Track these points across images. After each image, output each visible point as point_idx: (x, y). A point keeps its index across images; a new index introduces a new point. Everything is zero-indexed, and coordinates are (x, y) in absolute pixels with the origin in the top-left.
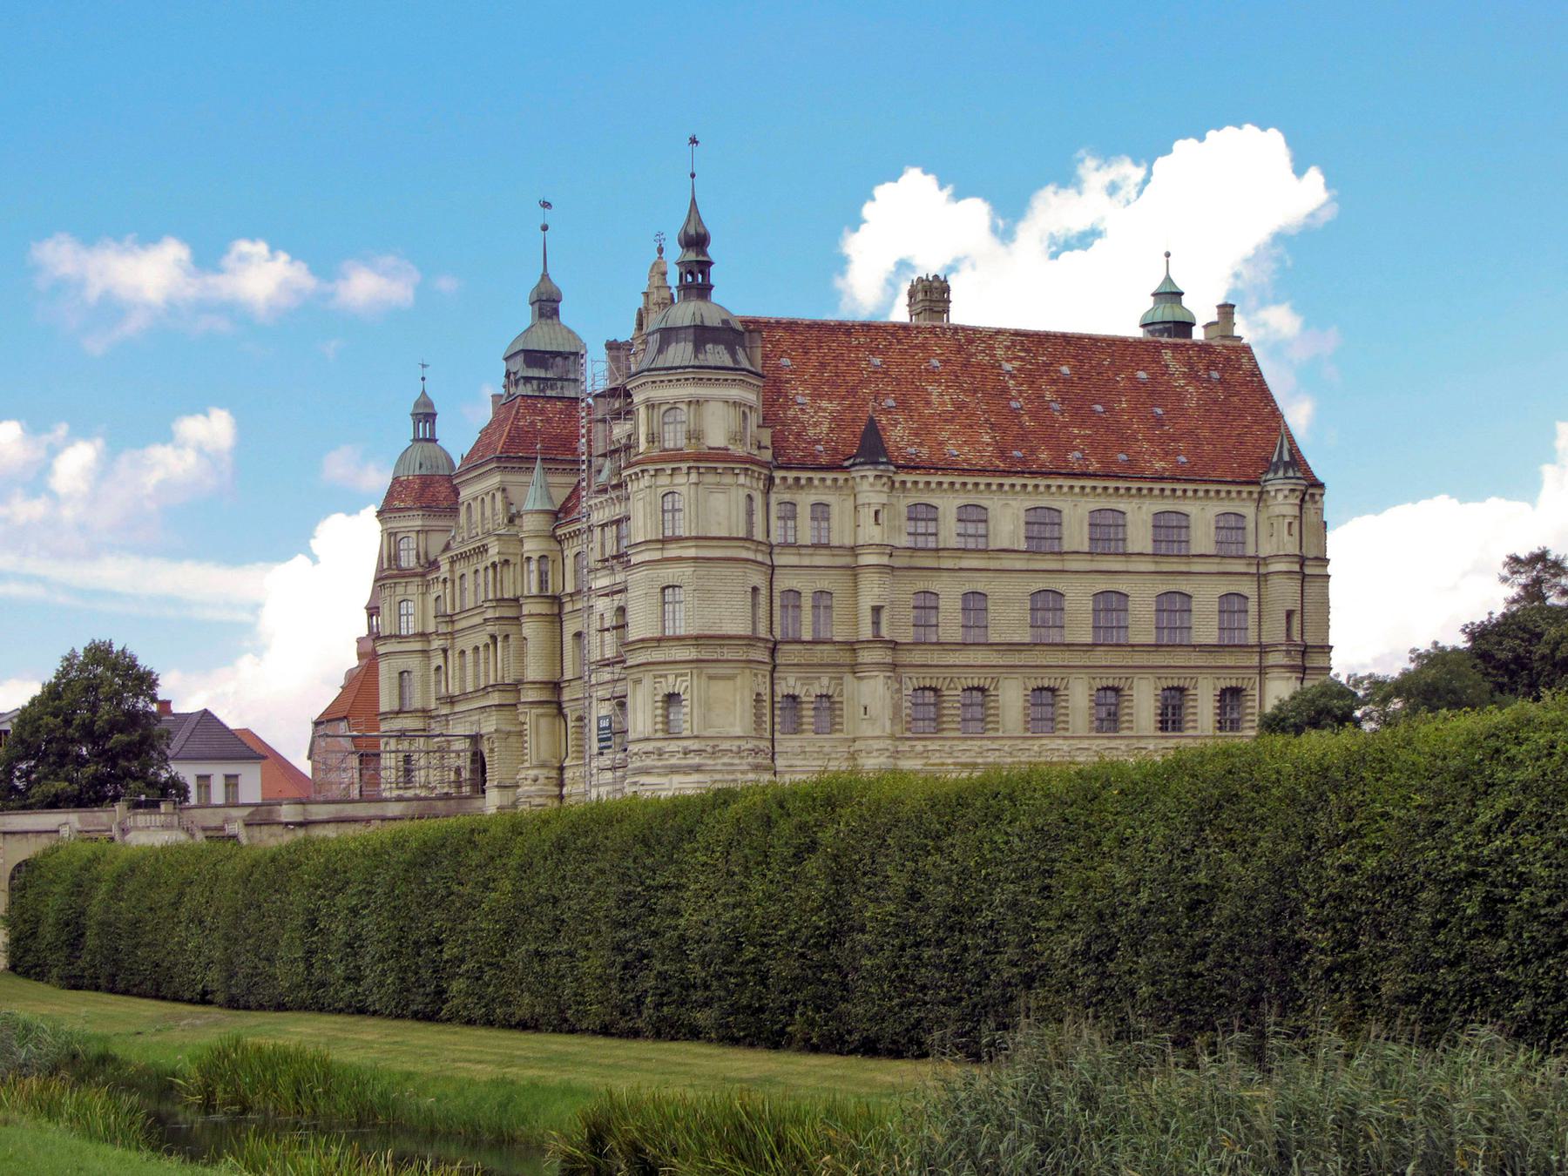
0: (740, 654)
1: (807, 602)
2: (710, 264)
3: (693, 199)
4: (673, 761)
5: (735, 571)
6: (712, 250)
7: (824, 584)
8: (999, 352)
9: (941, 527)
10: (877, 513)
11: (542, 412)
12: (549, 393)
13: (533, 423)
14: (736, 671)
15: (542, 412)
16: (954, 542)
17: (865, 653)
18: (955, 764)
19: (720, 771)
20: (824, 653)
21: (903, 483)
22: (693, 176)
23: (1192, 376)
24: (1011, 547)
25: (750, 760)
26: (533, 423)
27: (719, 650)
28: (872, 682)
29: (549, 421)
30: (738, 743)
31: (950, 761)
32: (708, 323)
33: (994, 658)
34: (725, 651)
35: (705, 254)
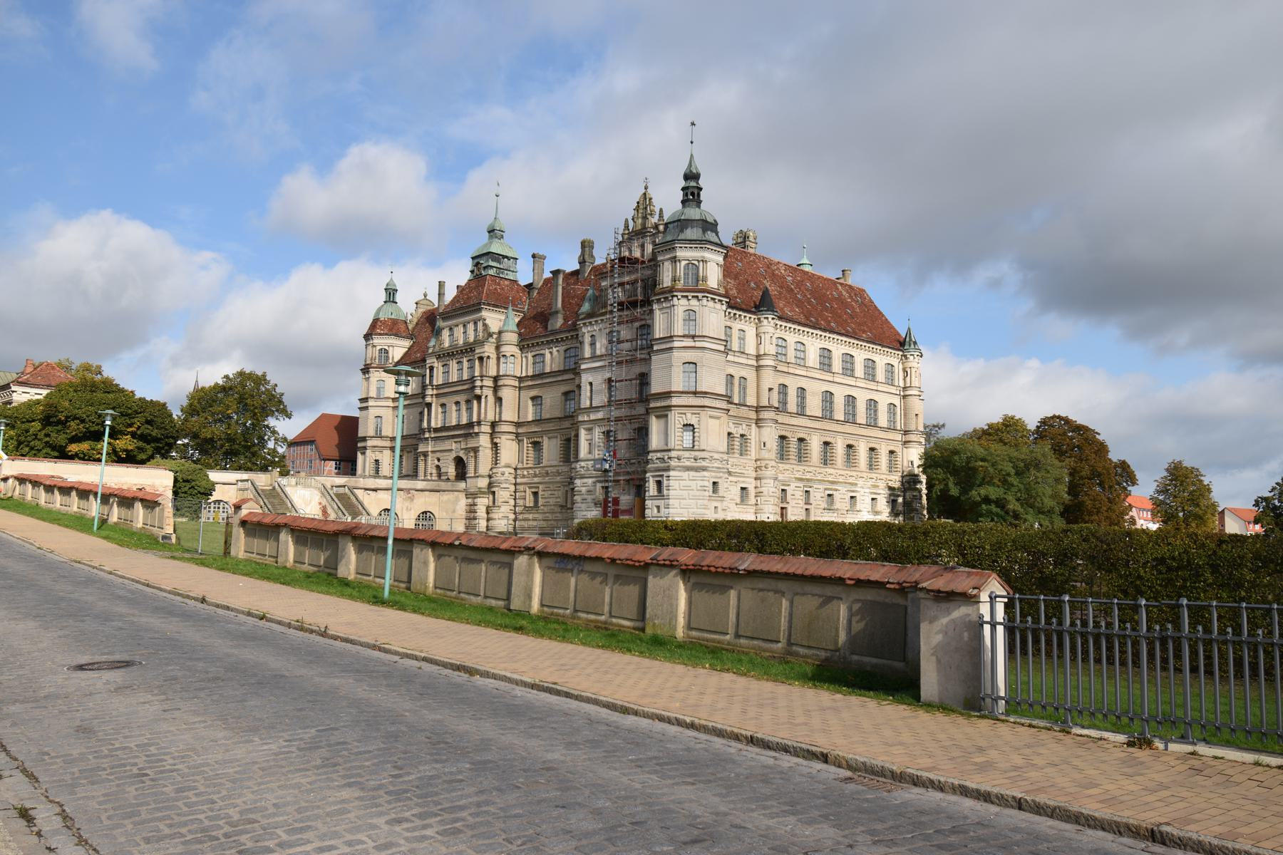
1: (736, 382)
2: (701, 189)
3: (692, 155)
4: (688, 464)
6: (702, 182)
7: (744, 373)
8: (783, 272)
9: (789, 351)
11: (499, 284)
12: (501, 276)
13: (496, 289)
15: (499, 284)
16: (793, 360)
17: (766, 413)
19: (714, 472)
20: (744, 411)
22: (692, 142)
23: (851, 297)
26: (496, 289)
28: (769, 429)
29: (503, 289)
32: (708, 220)
35: (698, 183)
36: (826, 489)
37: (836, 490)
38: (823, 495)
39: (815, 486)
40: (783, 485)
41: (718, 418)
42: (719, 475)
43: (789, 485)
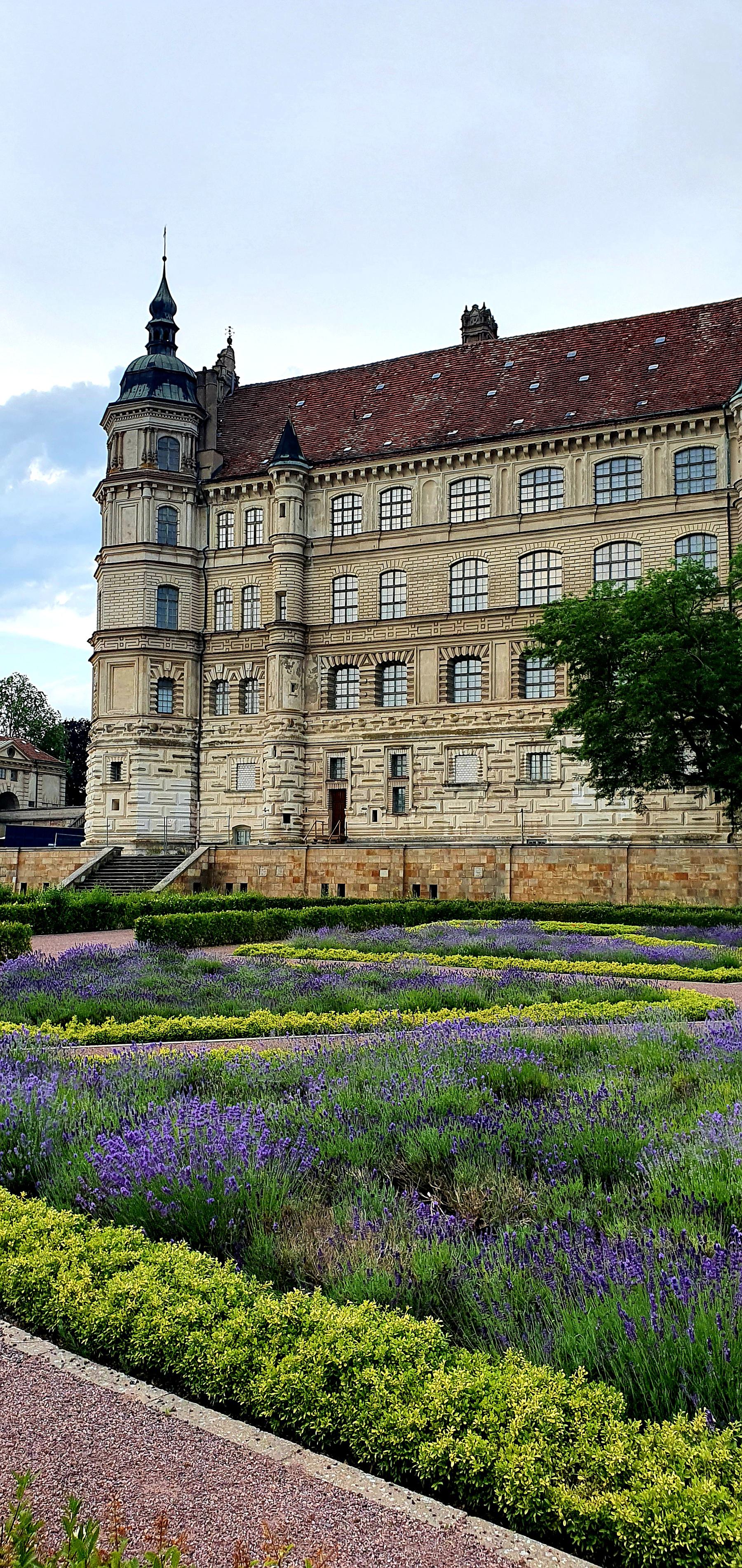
0: (137, 643)
5: (140, 571)
10: (283, 506)
14: (131, 659)
18: (364, 736)
19: (113, 747)
20: (247, 639)
21: (322, 478)
24: (435, 523)
25: (142, 736)
27: (119, 642)
30: (130, 721)
31: (361, 733)
33: (407, 632)
34: (124, 641)
36: (448, 747)
37: (481, 746)
38: (441, 759)
39: (416, 745)
40: (333, 751)
41: (130, 665)
42: (120, 751)
43: (346, 750)
